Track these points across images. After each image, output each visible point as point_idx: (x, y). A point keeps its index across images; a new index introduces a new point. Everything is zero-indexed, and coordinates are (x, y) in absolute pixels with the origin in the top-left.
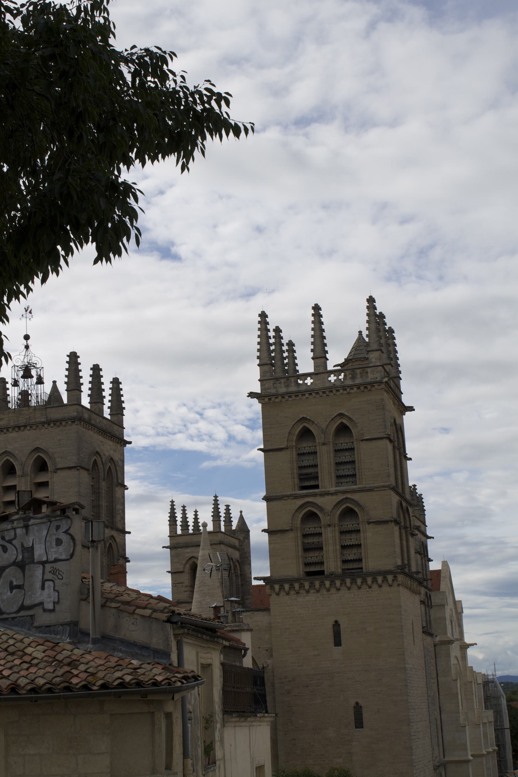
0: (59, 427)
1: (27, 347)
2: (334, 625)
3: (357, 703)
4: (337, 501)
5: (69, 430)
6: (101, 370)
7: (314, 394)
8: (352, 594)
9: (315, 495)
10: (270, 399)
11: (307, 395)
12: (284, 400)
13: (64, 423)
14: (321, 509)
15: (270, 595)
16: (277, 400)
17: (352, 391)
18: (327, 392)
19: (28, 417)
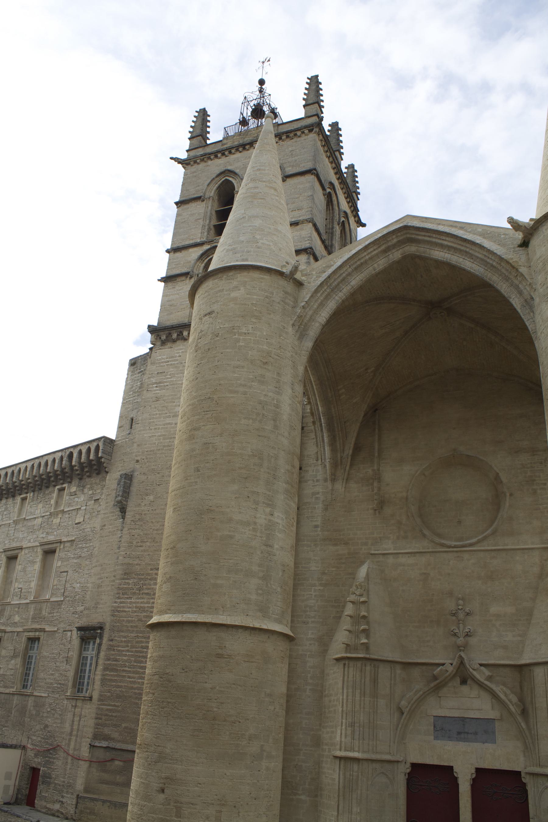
0: (292, 139)
1: (261, 90)
5: (305, 139)
6: (340, 129)
13: (299, 133)
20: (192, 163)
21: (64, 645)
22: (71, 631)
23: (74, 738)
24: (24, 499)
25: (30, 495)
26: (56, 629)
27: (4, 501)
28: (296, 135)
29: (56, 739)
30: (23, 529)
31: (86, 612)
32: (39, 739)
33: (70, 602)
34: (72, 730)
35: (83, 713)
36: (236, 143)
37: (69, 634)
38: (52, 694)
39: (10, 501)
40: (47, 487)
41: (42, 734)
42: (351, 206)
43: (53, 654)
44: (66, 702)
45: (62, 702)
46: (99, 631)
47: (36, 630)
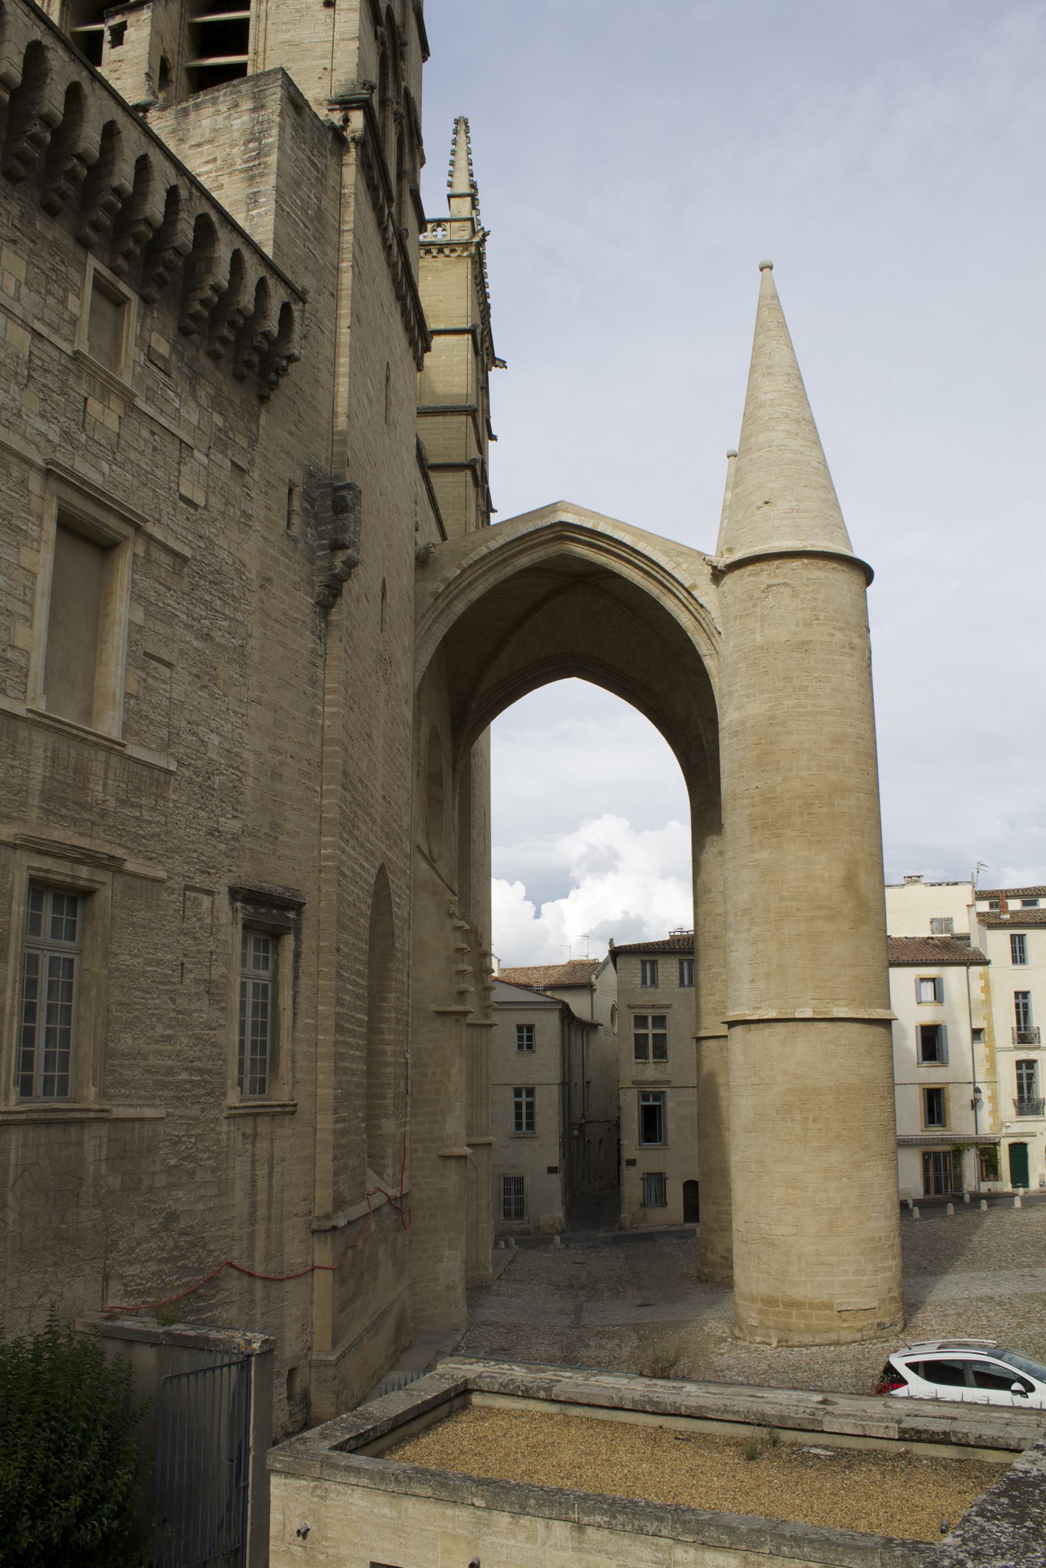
21: (195, 939)
22: (209, 893)
23: (261, 1228)
26: (162, 875)
29: (212, 1247)
31: (248, 842)
32: (153, 1267)
33: (196, 789)
34: (254, 1205)
35: (277, 1152)
37: (206, 901)
38: (177, 1107)
41: (162, 1249)
43: (159, 963)
44: (224, 1128)
45: (214, 1129)
46: (291, 915)
47: (89, 858)
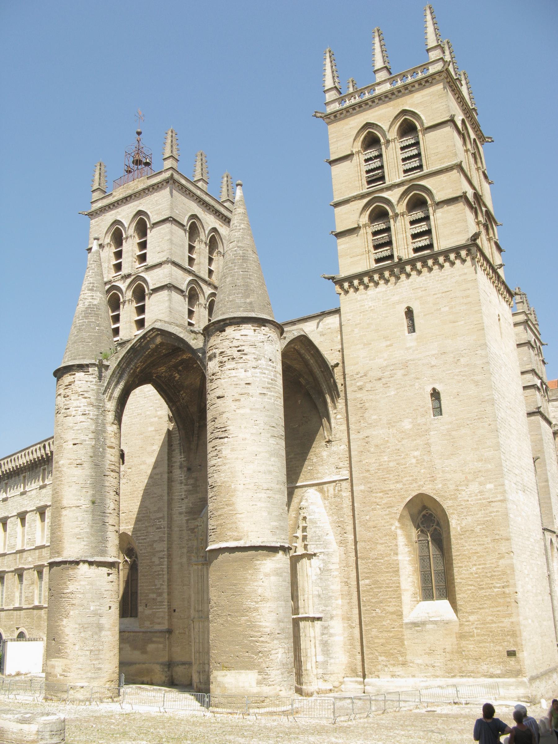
2: (406, 313)
3: (434, 389)
4: (404, 190)
7: (376, 101)
8: (424, 278)
9: (382, 190)
10: (335, 116)
11: (370, 103)
12: (348, 114)
14: (387, 201)
15: (340, 294)
16: (342, 116)
17: (413, 89)
18: (390, 96)
19: (133, 188)
20: (94, 214)
24: (24, 477)
25: (27, 474)
27: (13, 479)
28: (158, 186)
30: (27, 498)
36: (121, 196)
39: (17, 477)
40: (36, 468)
42: (222, 217)
